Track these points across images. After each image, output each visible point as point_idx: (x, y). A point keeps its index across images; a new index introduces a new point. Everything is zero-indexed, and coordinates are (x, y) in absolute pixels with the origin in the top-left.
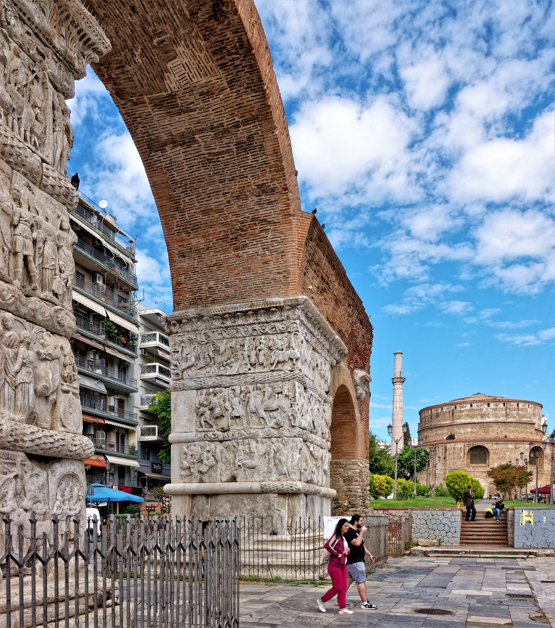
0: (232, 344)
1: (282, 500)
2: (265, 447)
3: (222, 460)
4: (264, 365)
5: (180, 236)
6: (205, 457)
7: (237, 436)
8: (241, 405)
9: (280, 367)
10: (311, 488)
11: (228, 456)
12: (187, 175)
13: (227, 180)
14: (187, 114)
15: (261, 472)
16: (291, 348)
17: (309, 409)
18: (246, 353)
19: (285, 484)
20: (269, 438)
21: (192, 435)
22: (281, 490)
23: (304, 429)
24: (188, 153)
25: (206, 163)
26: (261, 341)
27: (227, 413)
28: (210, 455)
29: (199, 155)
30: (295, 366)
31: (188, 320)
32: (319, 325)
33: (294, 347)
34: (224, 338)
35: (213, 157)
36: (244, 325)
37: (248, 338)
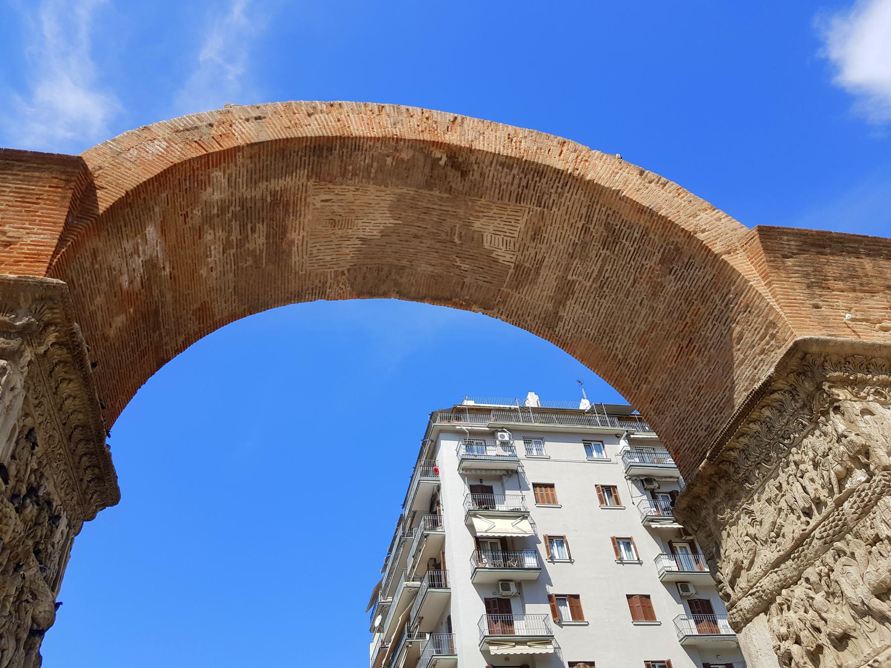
5: (643, 391)
12: (597, 321)
13: (631, 289)
14: (542, 267)
24: (579, 299)
25: (600, 292)
29: (588, 291)
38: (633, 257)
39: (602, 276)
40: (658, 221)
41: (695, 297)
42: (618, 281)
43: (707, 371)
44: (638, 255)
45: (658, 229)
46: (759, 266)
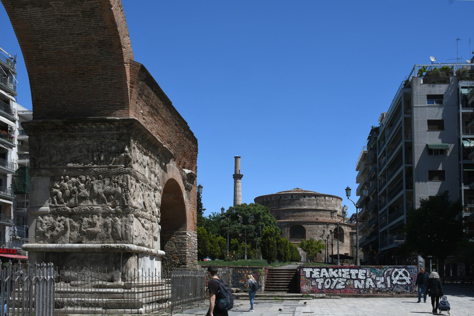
24: (44, 12)
35: (64, 18)
38: (90, 28)
39: (67, 18)
40: (114, 30)
41: (101, 64)
42: (72, 26)
43: (81, 89)
44: (93, 29)
45: (111, 32)
46: (132, 78)
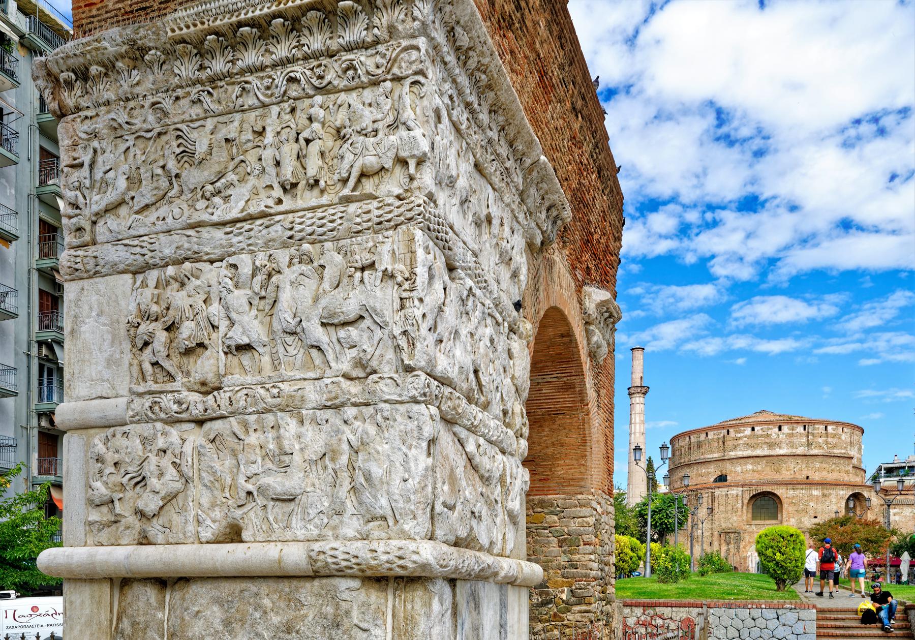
0: (231, 131)
1: (374, 596)
2: (323, 436)
3: (200, 478)
4: (322, 183)
6: (153, 468)
7: (242, 403)
8: (254, 312)
9: (368, 186)
10: (468, 560)
11: (217, 465)
15: (313, 512)
16: (402, 127)
17: (464, 332)
18: (268, 155)
19: (381, 548)
20: (336, 407)
21: (116, 407)
22: (371, 568)
23: (444, 381)
26: (312, 111)
27: (214, 336)
28: (166, 462)
30: (415, 184)
31: (104, 65)
32: (491, 95)
33: (411, 124)
34: (208, 114)
36: (262, 68)
37: (275, 109)
